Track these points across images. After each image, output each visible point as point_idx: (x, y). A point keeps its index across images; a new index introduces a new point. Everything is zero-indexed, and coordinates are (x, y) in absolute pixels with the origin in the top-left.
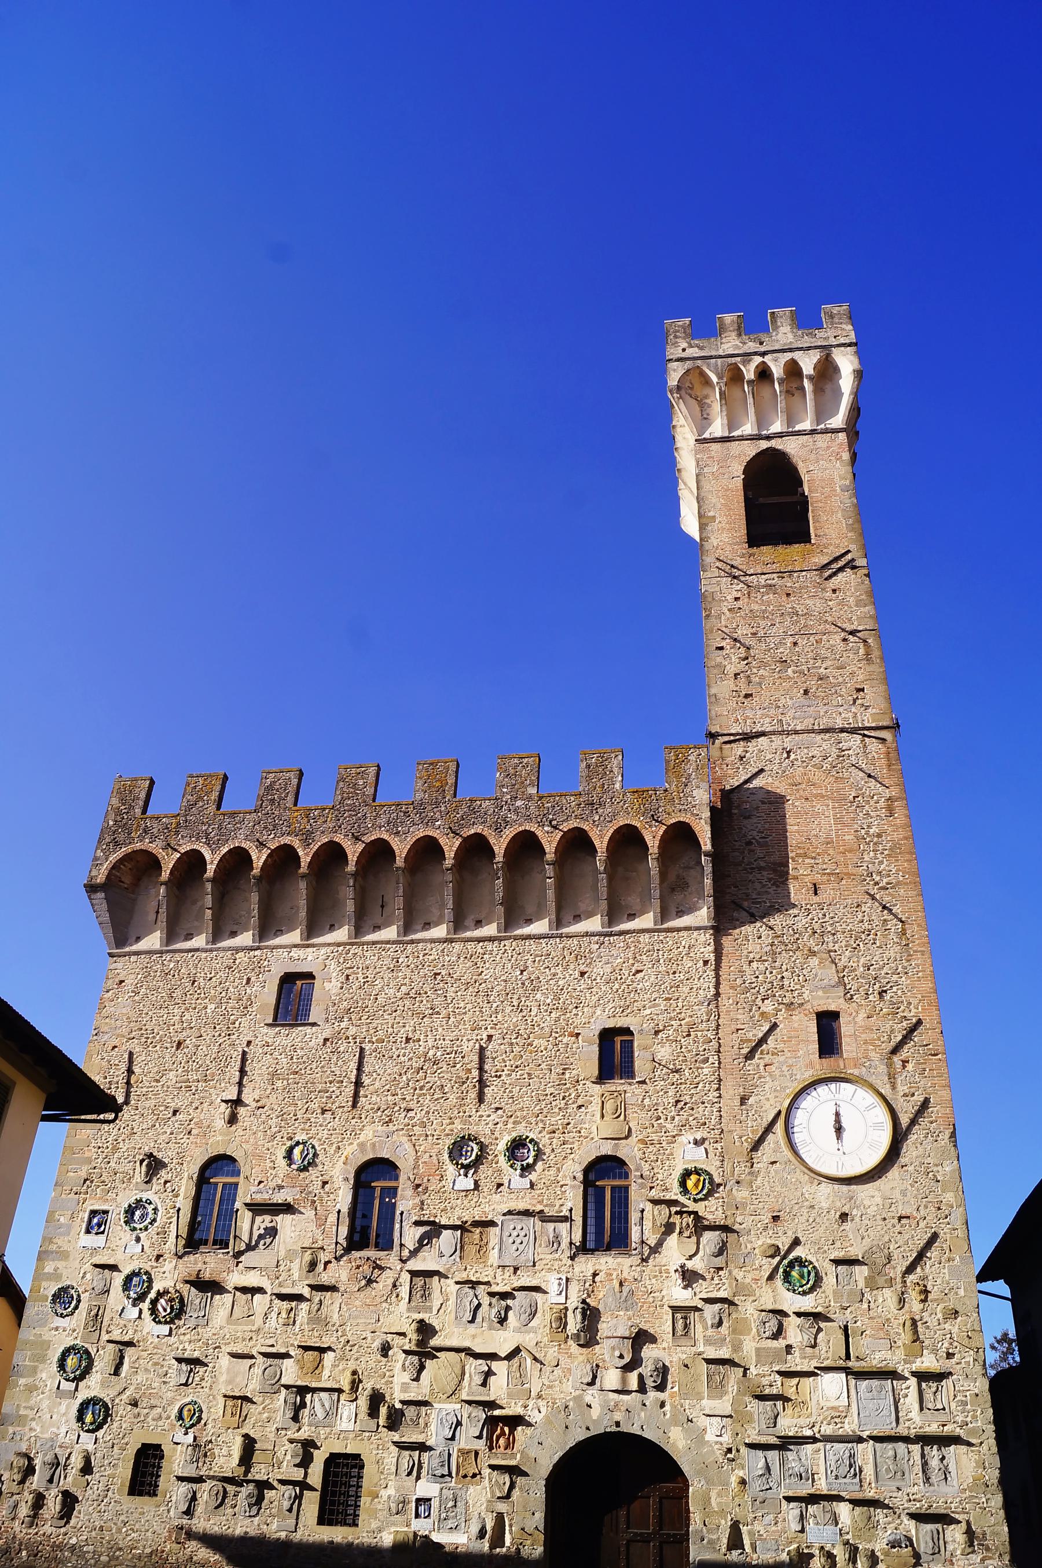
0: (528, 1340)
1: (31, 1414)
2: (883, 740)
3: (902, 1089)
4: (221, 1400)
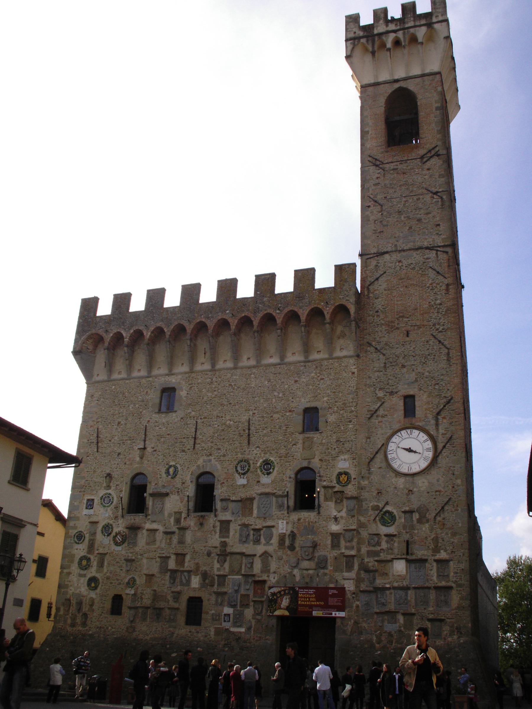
0: (270, 549)
1: (70, 584)
3: (441, 431)
4: (144, 576)
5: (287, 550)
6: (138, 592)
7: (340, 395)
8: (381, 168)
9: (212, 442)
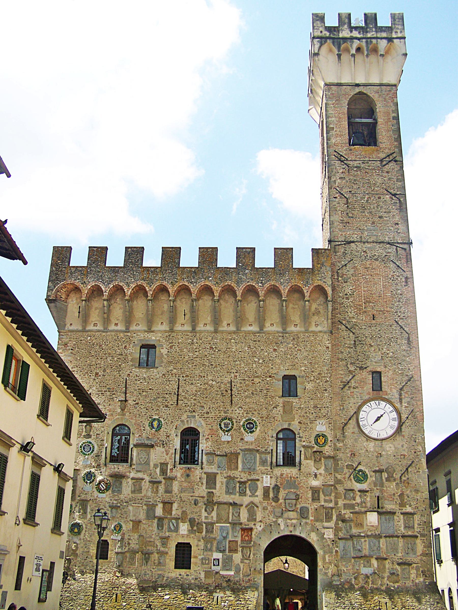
2: (405, 249)
3: (404, 404)
5: (272, 501)
6: (125, 537)
7: (316, 366)
8: (346, 164)
9: (195, 400)
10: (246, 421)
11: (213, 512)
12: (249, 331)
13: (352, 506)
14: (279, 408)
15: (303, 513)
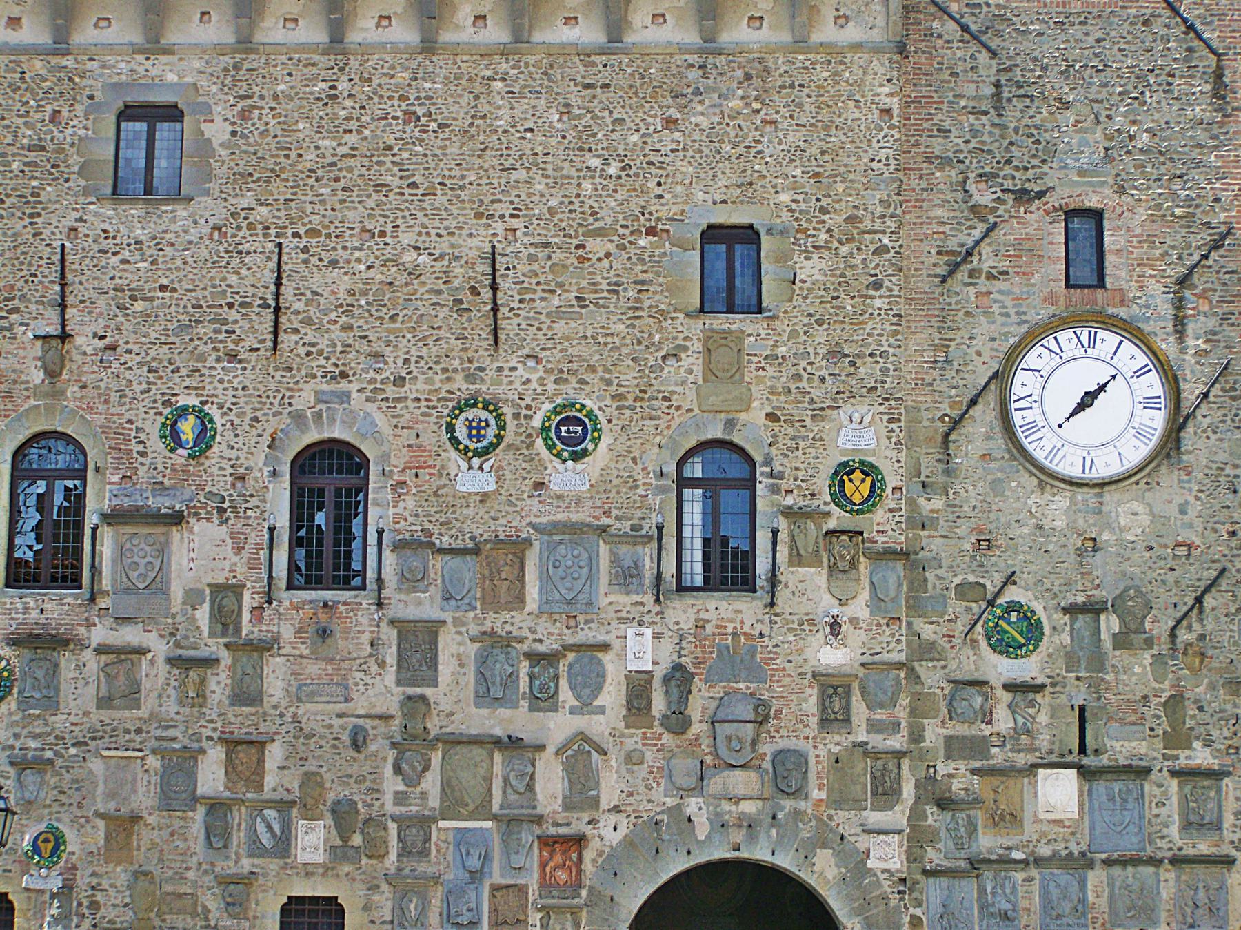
5: (660, 730)
6: (79, 882)
7: (840, 187)
9: (347, 328)
10: (555, 411)
11: (429, 776)
12: (563, 45)
13: (978, 747)
14: (687, 360)
15: (786, 775)
